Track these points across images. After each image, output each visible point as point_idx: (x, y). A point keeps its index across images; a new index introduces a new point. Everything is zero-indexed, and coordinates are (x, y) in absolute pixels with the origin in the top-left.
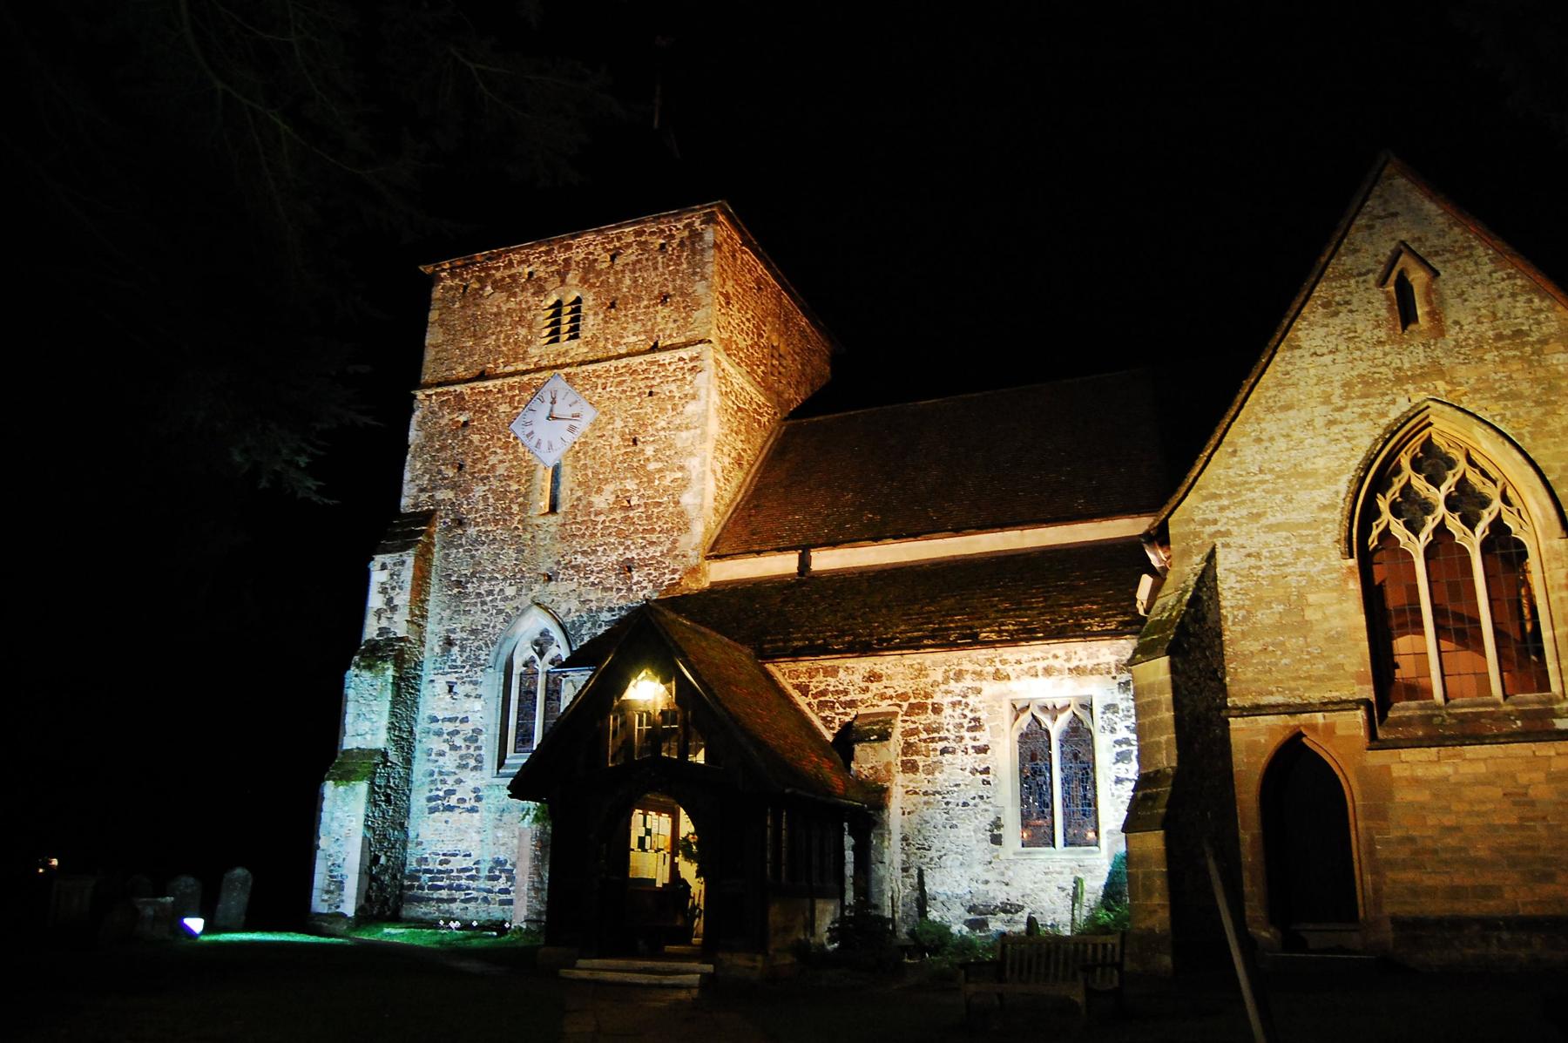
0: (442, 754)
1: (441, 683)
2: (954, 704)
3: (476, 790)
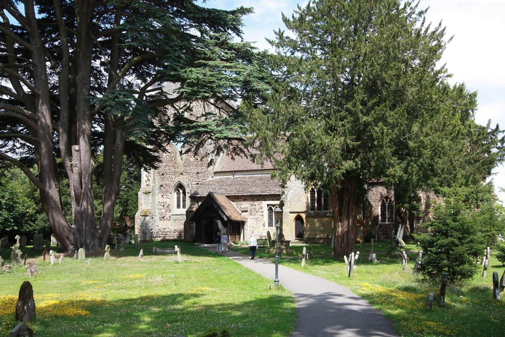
0: (161, 209)
1: (160, 195)
2: (258, 205)
3: (170, 216)
